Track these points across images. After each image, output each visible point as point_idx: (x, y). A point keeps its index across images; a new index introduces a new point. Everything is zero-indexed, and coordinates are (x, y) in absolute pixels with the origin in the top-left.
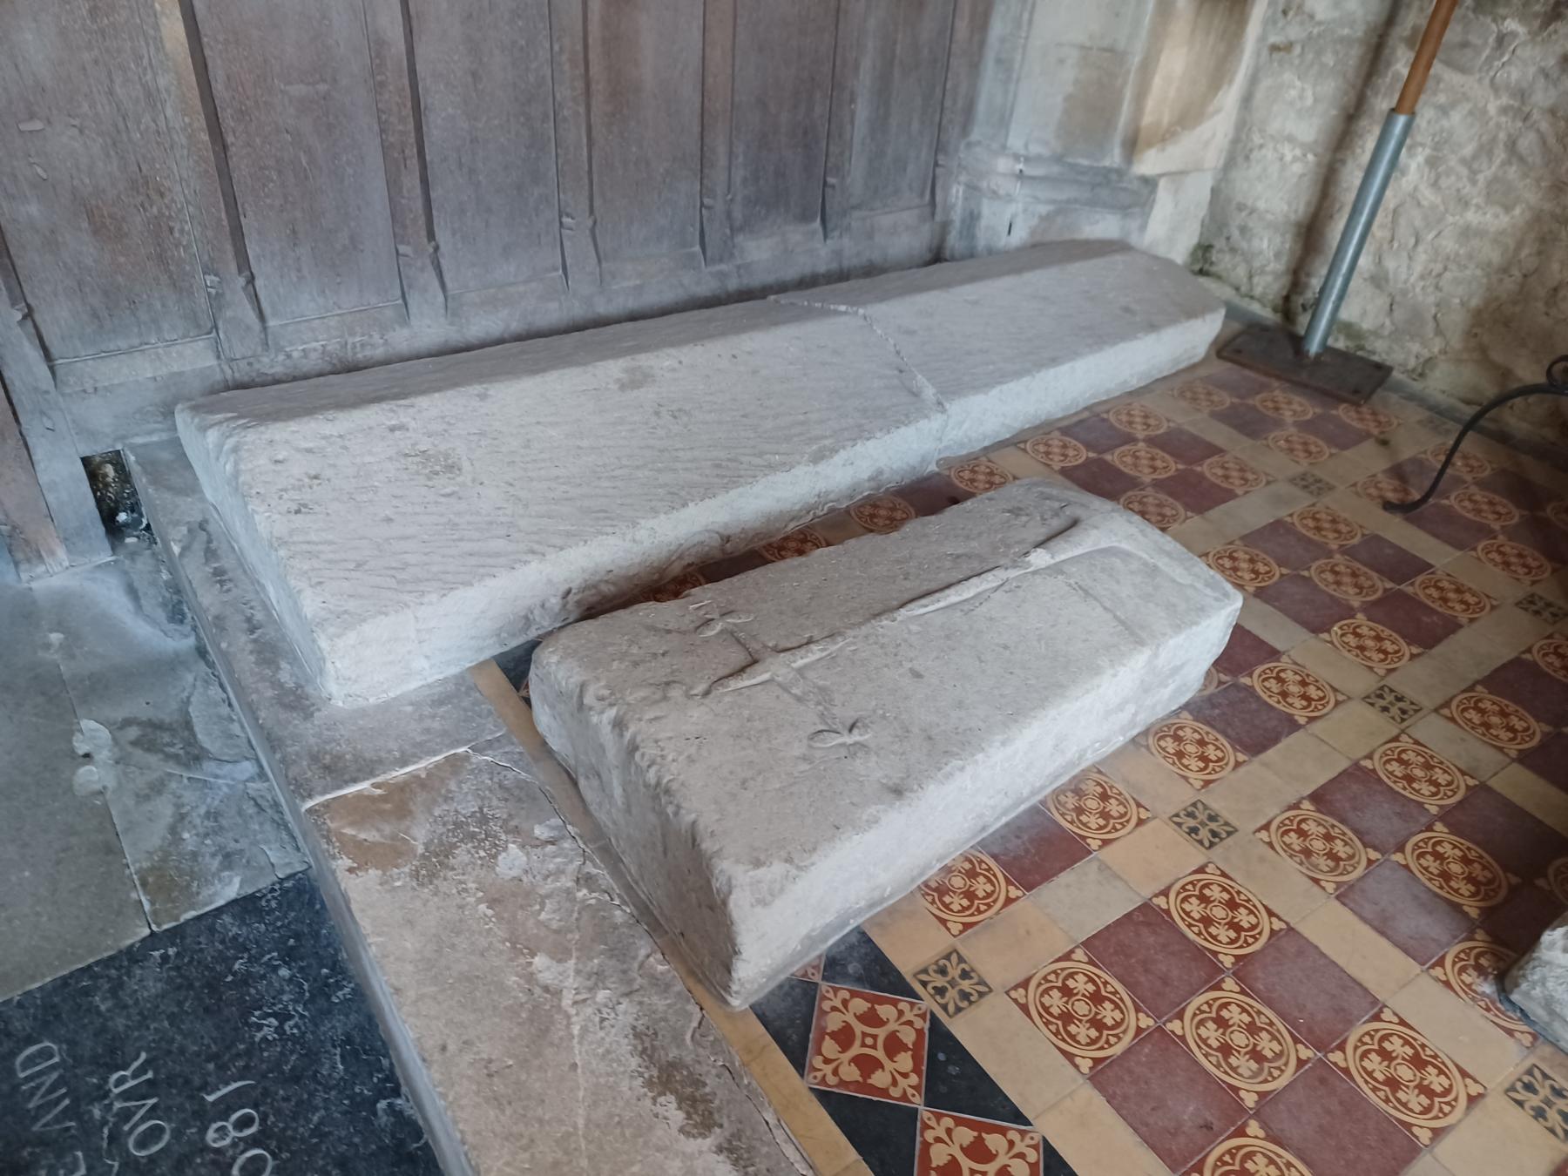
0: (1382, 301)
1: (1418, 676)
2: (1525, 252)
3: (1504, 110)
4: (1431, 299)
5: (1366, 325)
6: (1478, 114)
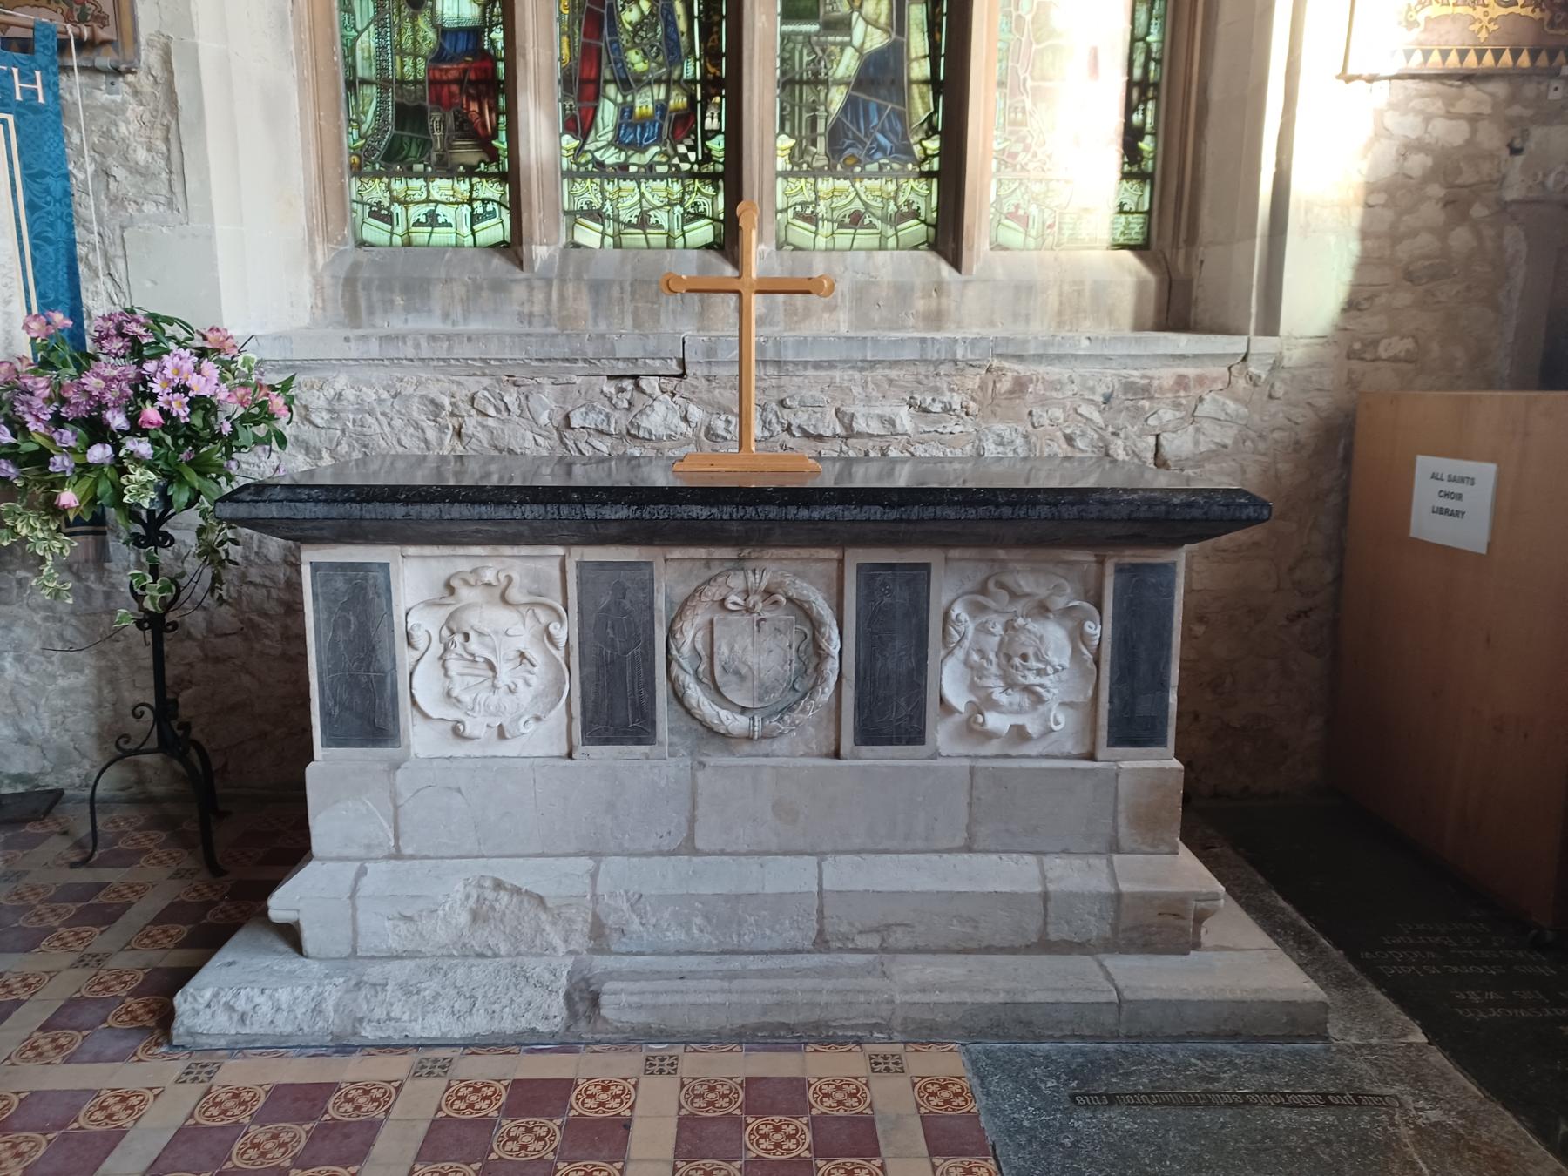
0: (35, 751)
1: (102, 940)
2: (106, 691)
3: (46, 619)
4: (66, 738)
5: (32, 771)
6: (31, 625)
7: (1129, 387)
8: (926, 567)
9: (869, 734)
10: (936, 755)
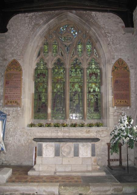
7: (98, 131)
8: (78, 144)
9: (75, 156)
10: (79, 157)
